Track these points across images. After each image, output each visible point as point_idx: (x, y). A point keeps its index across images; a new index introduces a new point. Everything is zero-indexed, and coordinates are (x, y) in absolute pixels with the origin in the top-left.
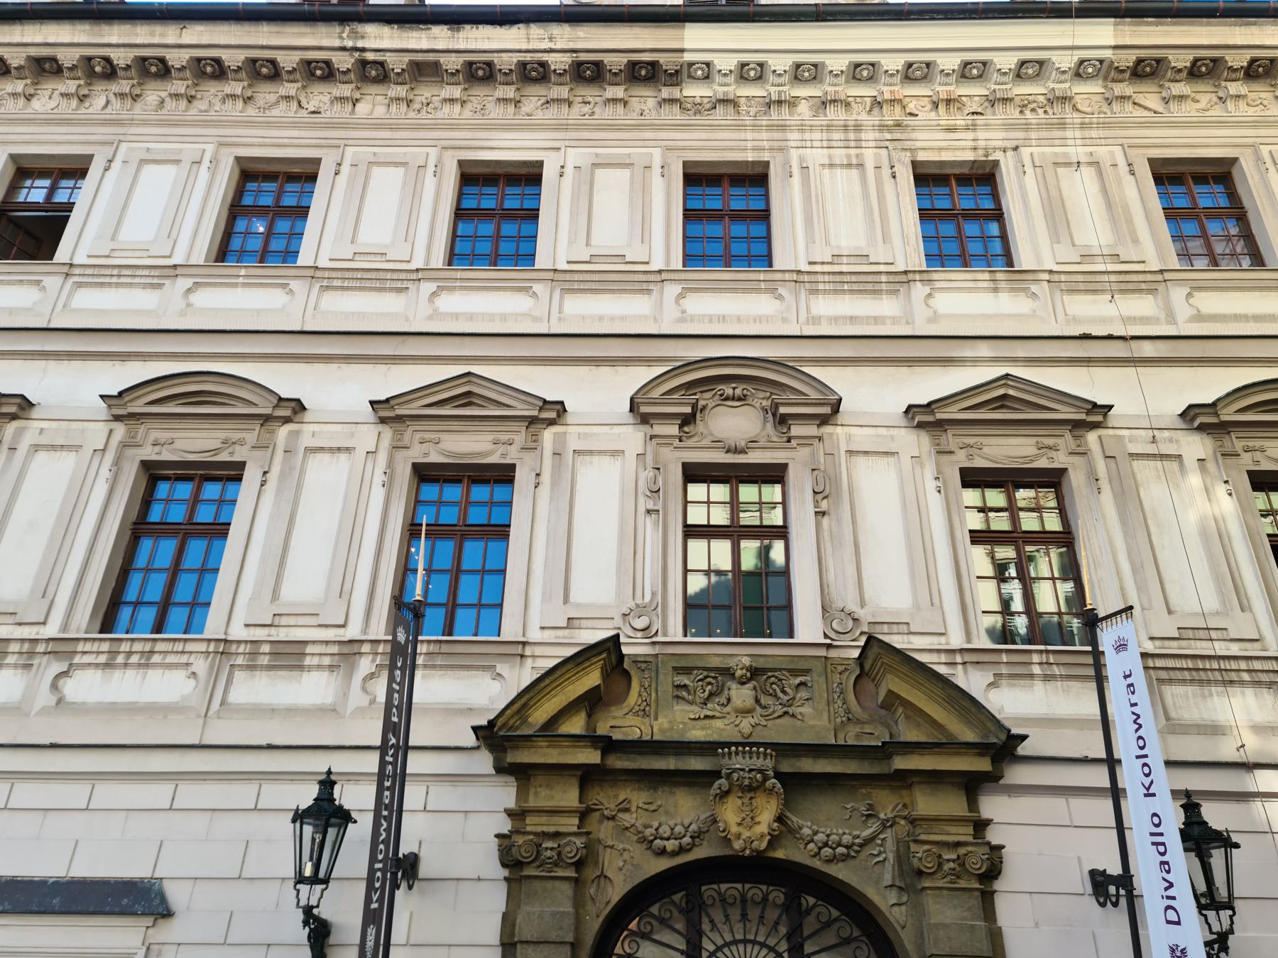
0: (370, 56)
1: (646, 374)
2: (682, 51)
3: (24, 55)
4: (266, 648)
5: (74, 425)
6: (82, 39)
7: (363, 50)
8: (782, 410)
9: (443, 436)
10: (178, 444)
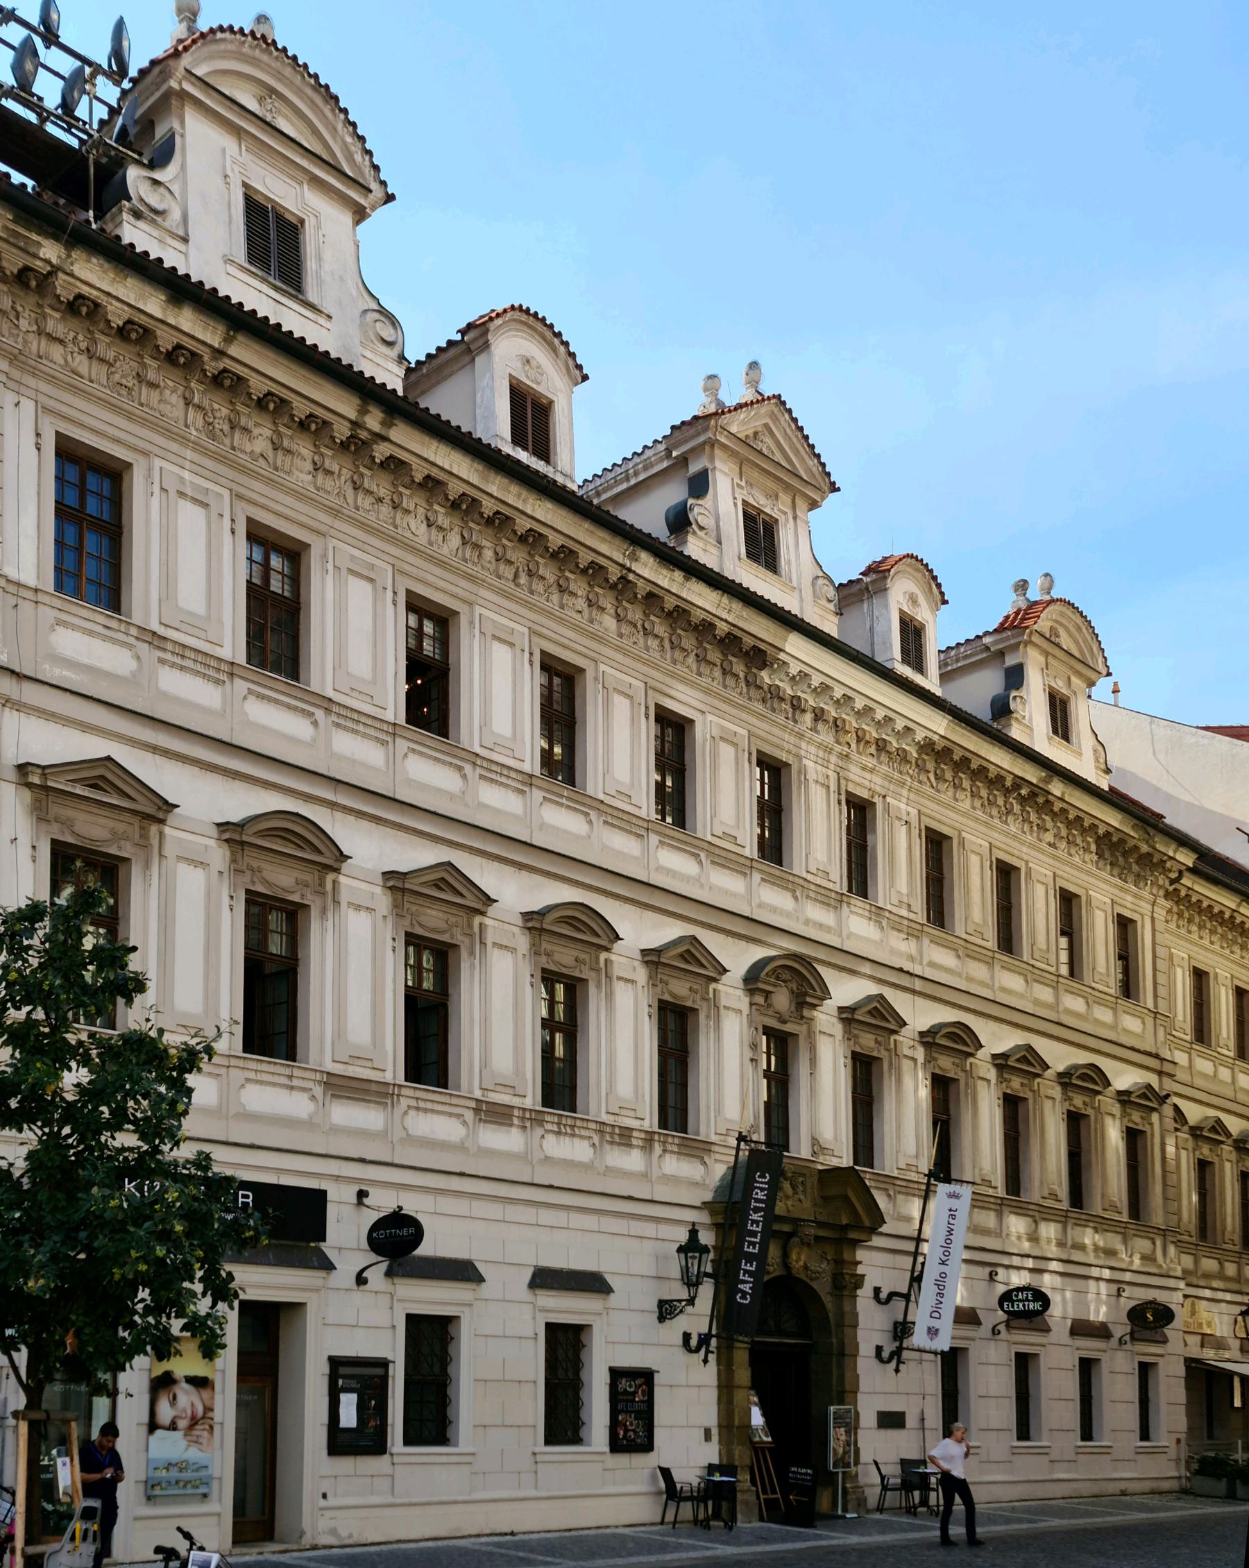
0: (631, 577)
1: (759, 953)
2: (781, 650)
3: (426, 472)
4: (617, 1131)
5: (506, 926)
6: (474, 479)
7: (630, 570)
8: (809, 999)
9: (671, 980)
10: (557, 957)
